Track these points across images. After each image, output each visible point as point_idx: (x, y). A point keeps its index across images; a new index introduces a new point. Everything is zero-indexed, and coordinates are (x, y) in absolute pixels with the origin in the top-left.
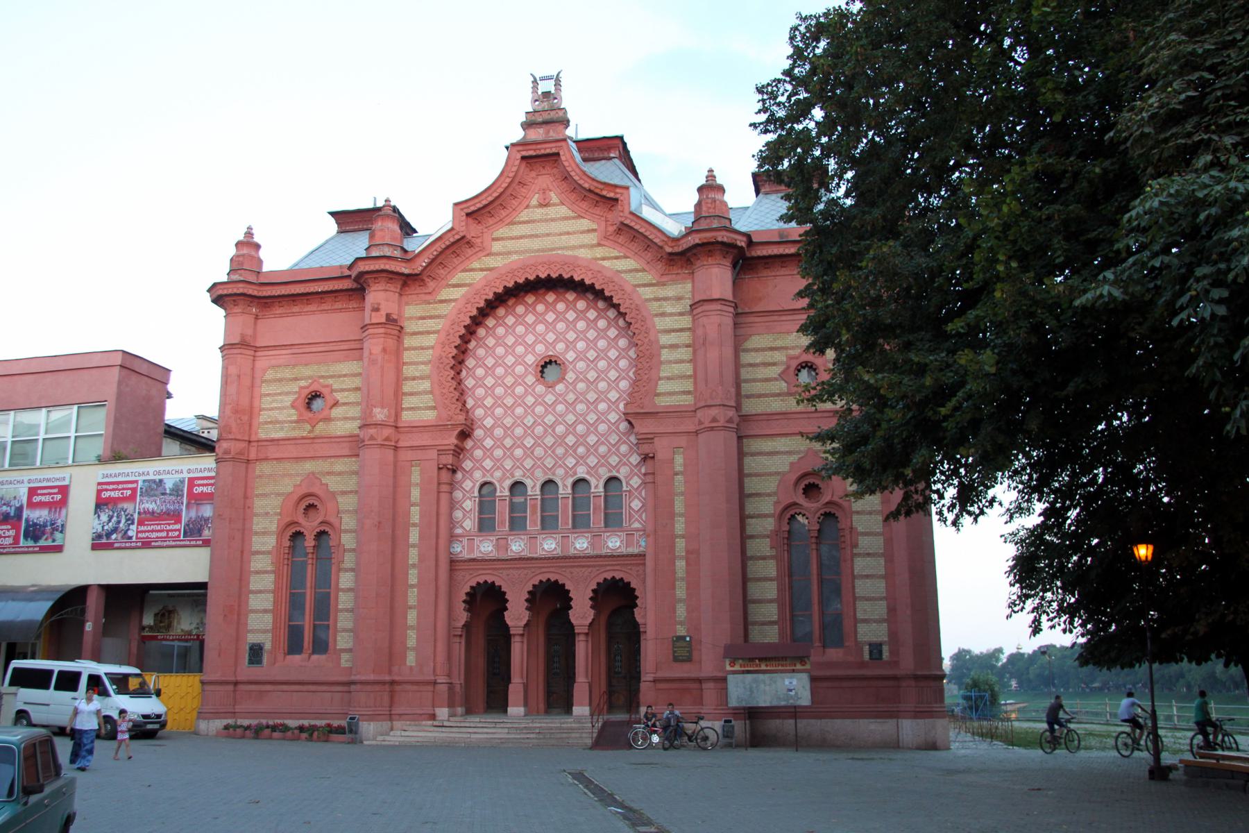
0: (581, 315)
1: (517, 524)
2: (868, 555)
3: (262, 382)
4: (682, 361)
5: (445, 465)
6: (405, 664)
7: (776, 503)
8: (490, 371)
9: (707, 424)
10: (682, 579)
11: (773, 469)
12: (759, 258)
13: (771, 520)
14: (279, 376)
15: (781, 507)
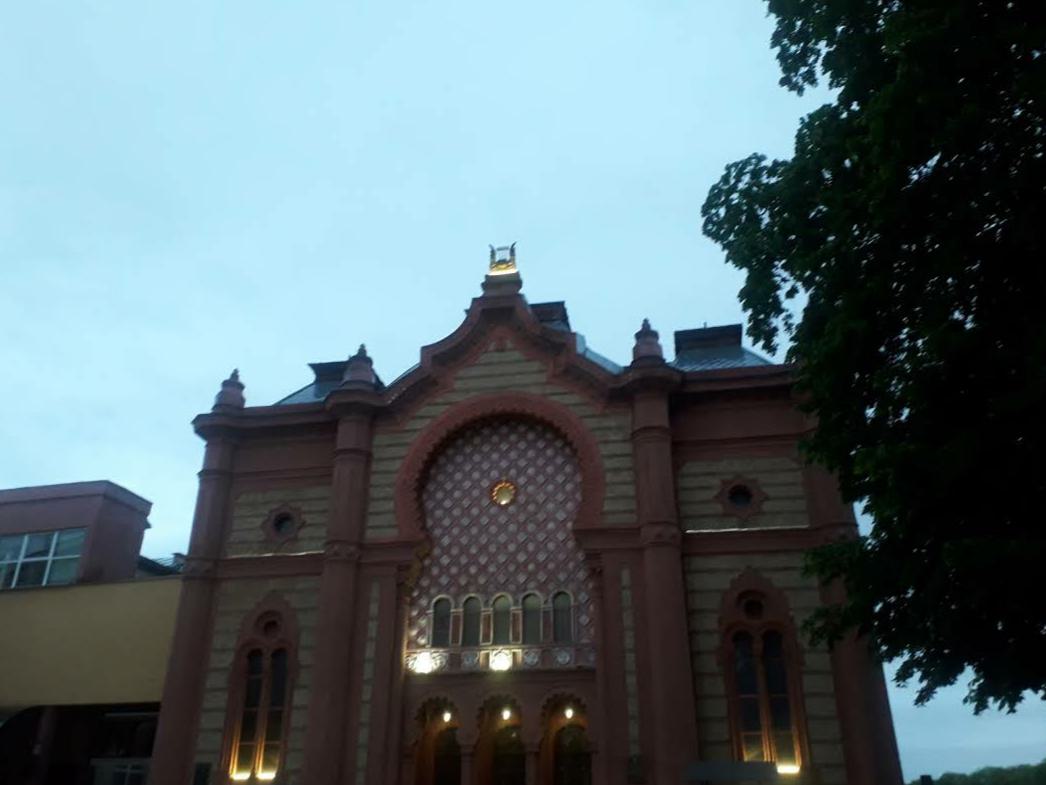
0: (531, 445)
4: (625, 483)
7: (720, 621)
8: (448, 494)
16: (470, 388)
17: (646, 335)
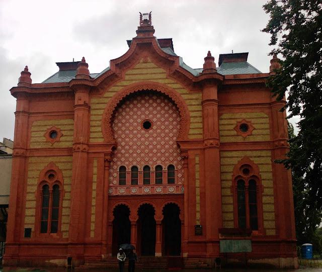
0: (159, 105)
1: (134, 182)
2: (268, 195)
3: (33, 126)
5: (107, 160)
6: (90, 236)
9: (209, 146)
10: (198, 203)
11: (232, 163)
12: (227, 85)
13: (231, 182)
14: (39, 124)
15: (235, 177)
16: (133, 79)
17: (209, 58)
